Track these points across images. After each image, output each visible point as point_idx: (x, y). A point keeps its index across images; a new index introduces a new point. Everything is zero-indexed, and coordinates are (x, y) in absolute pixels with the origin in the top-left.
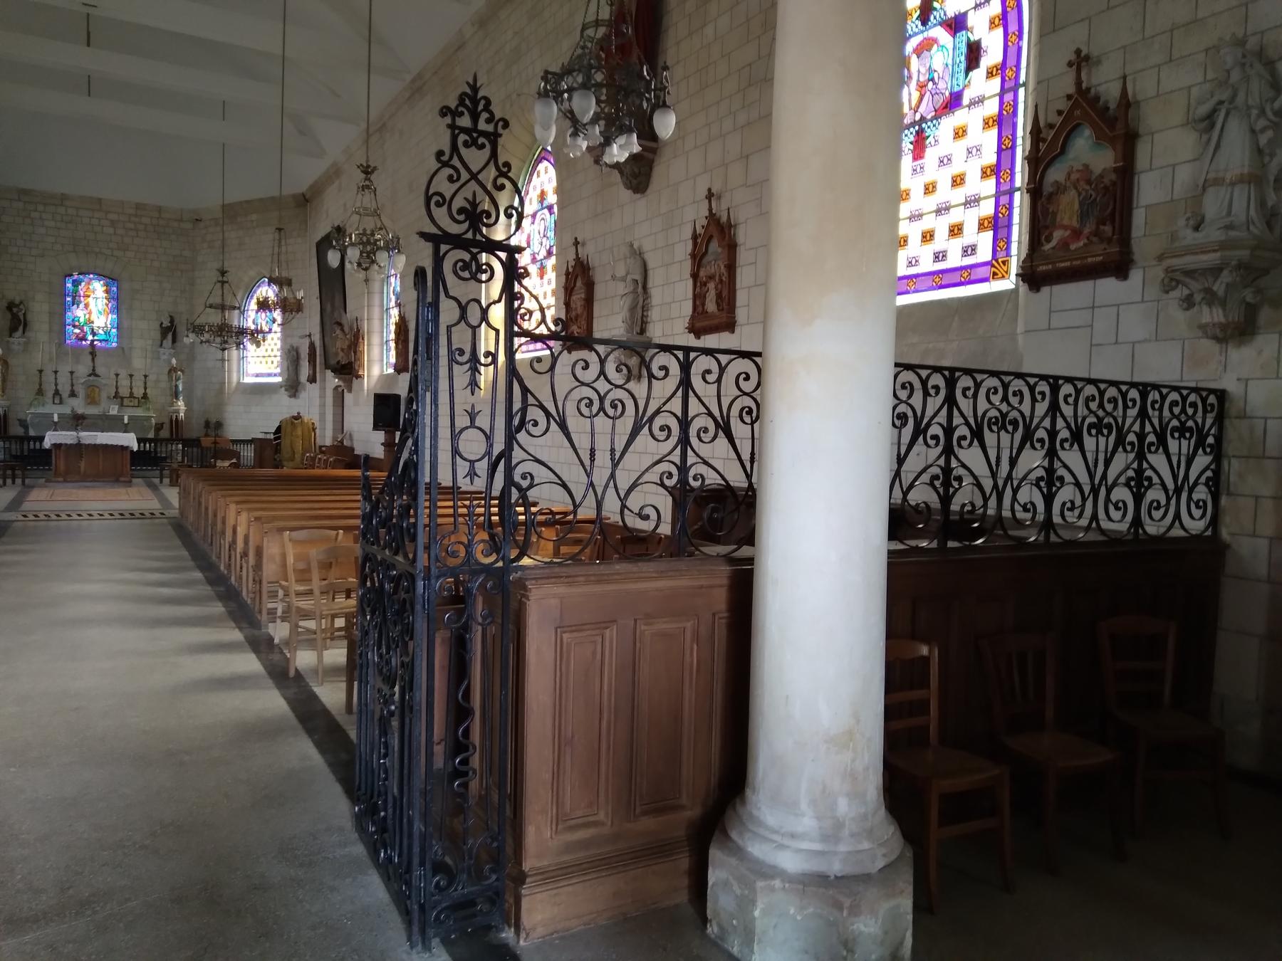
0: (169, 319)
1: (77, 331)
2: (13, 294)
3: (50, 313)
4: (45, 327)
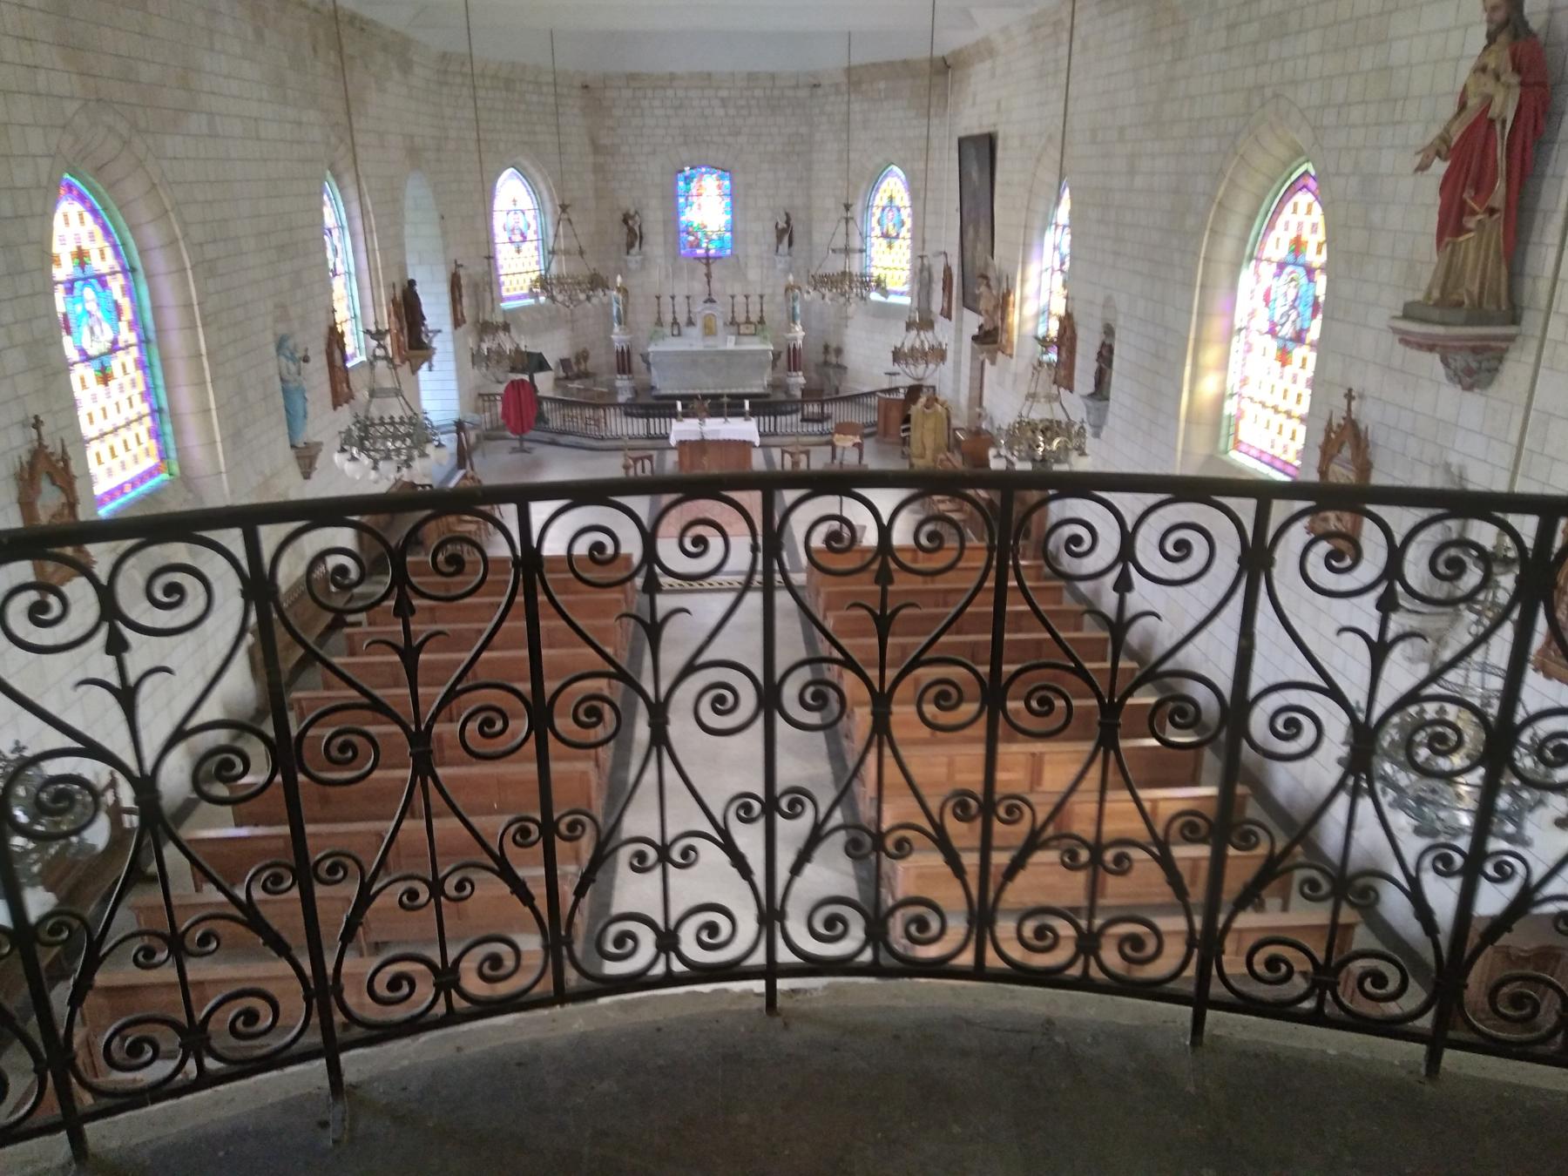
0: (785, 218)
1: (691, 238)
2: (627, 204)
4: (660, 239)
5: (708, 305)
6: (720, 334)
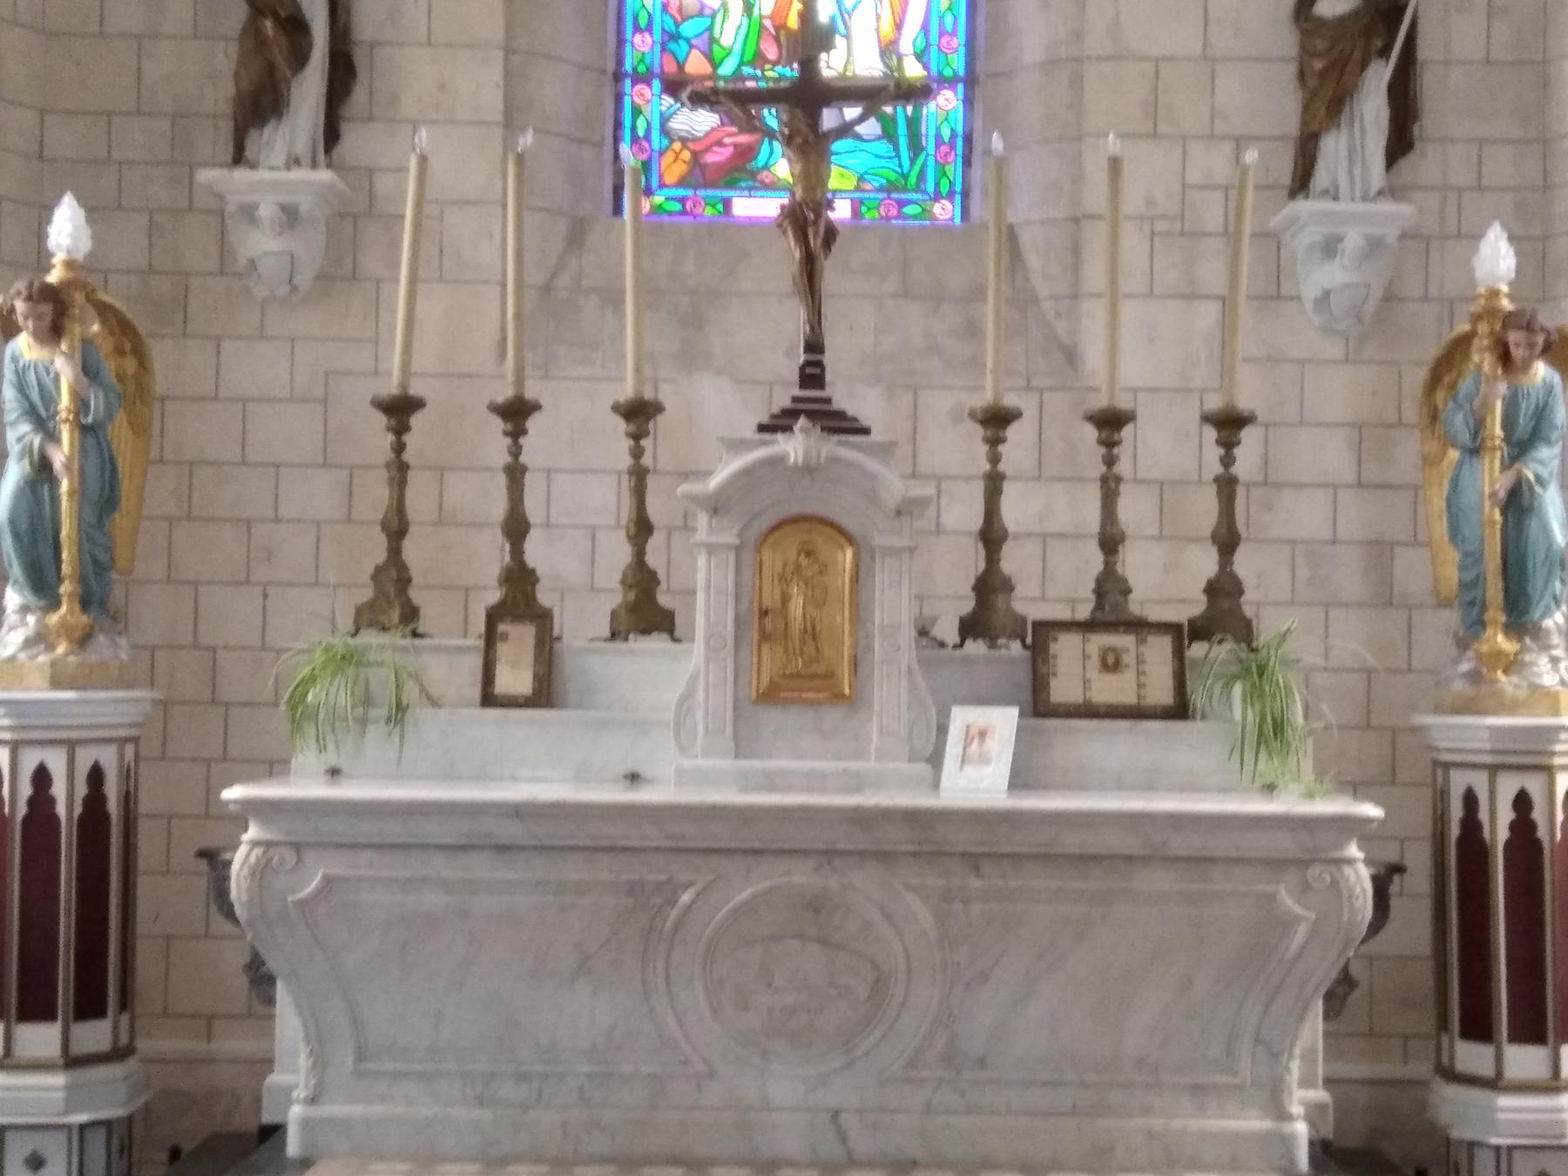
5: (794, 446)
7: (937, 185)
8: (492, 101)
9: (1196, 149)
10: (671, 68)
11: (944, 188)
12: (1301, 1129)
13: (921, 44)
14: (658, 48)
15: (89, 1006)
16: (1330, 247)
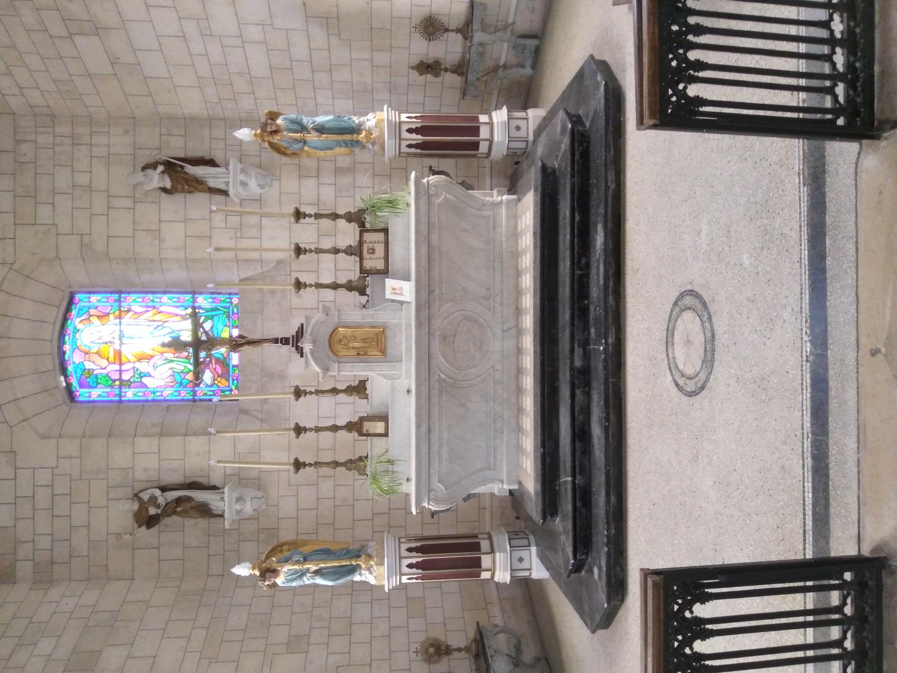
3: (161, 435)
4: (197, 444)
5: (307, 347)
6: (381, 316)
7: (228, 303)
8: (202, 439)
9: (214, 224)
10: (191, 384)
11: (228, 300)
12: (505, 197)
13: (182, 308)
14: (185, 389)
15: (476, 547)
16: (244, 184)
